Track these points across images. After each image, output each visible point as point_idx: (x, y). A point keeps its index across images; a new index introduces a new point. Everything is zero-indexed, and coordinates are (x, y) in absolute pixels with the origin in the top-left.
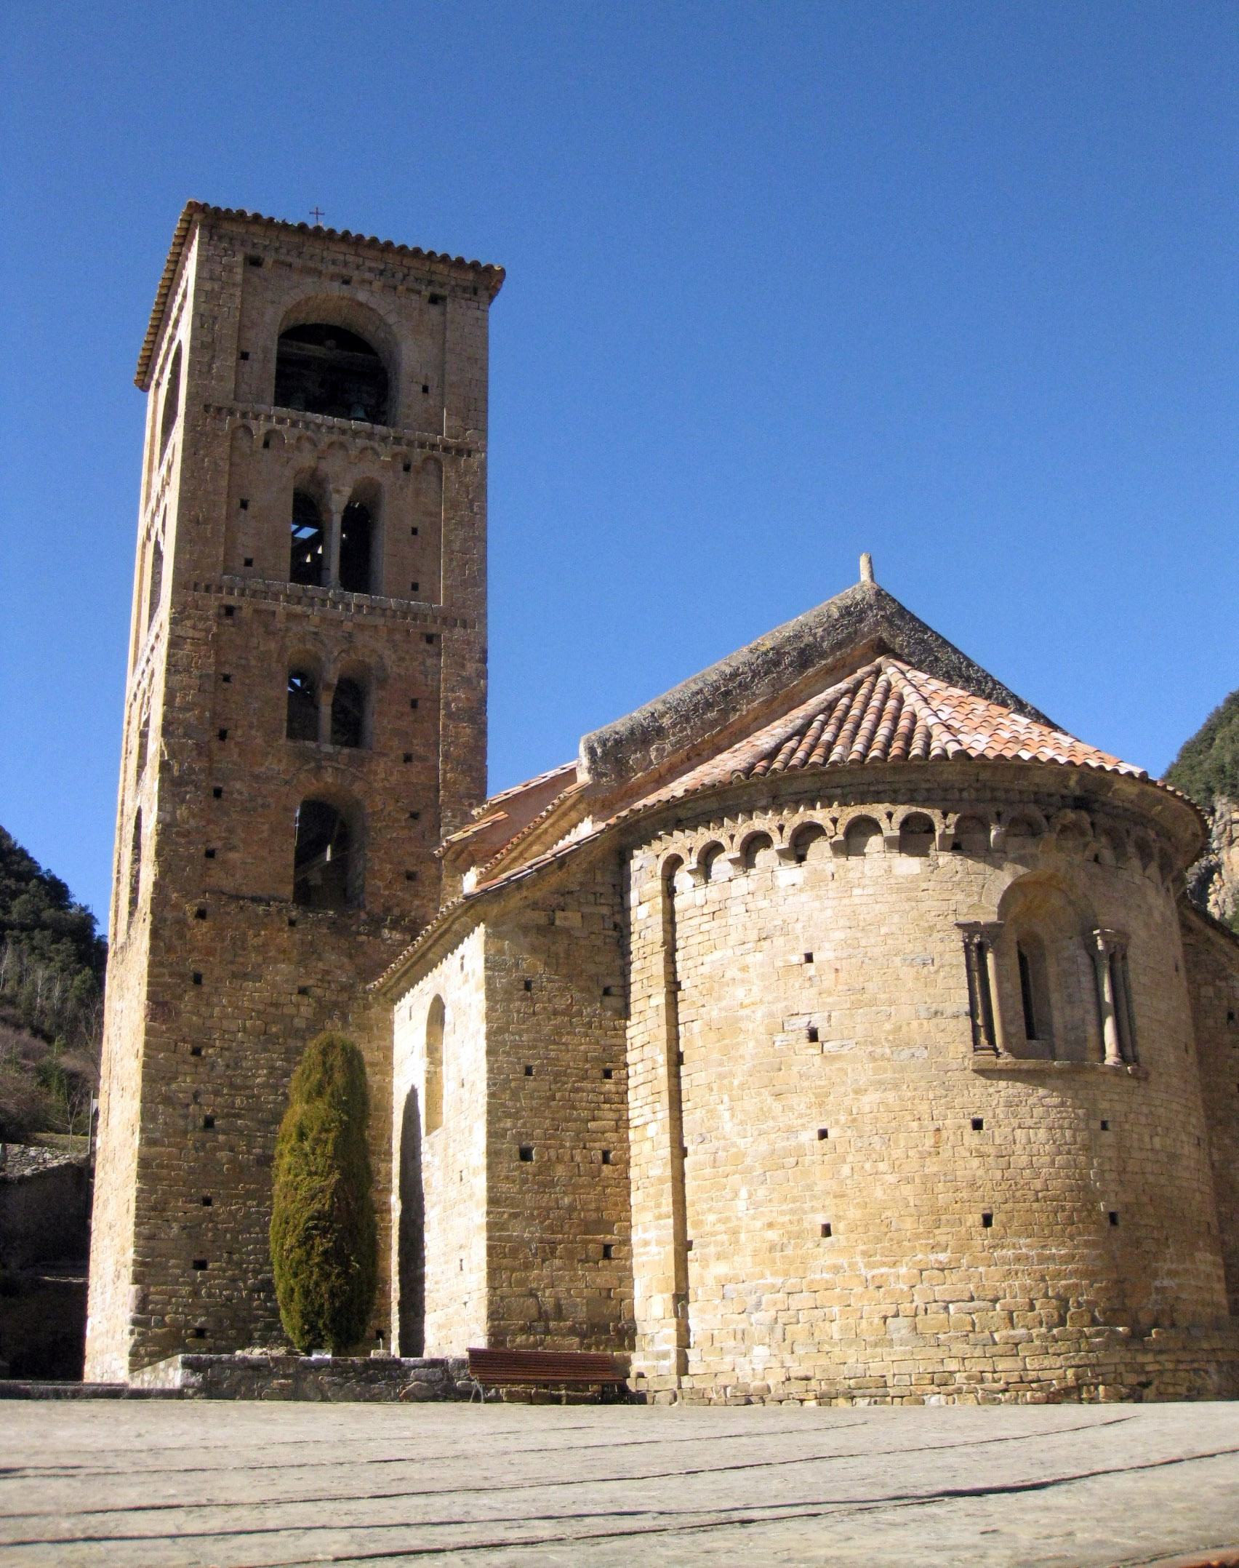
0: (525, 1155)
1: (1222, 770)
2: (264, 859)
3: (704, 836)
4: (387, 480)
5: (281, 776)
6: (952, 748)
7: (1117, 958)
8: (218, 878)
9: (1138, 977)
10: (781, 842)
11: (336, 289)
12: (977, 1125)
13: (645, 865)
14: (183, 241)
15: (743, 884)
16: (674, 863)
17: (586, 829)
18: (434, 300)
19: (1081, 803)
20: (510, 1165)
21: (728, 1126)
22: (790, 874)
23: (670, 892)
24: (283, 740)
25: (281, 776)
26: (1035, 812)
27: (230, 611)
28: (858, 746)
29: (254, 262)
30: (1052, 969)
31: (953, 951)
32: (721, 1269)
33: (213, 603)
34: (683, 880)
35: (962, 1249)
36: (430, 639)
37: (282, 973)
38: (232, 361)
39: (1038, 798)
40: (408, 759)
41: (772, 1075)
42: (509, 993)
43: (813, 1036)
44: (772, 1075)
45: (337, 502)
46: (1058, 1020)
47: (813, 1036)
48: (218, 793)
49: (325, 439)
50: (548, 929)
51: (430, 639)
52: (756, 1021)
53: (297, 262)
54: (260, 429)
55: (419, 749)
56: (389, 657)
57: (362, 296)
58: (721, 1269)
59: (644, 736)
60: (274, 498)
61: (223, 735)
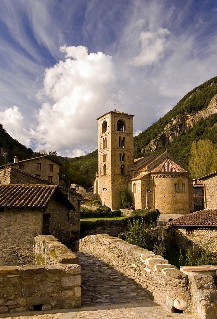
0: (144, 196)
1: (186, 107)
2: (118, 171)
3: (156, 175)
4: (126, 137)
5: (119, 164)
6: (175, 171)
7: (184, 185)
8: (116, 173)
9: (185, 186)
10: (162, 176)
11: (121, 118)
12: (175, 196)
13: (152, 176)
14: (109, 113)
15: (159, 179)
16: (154, 176)
17: (147, 173)
18: (129, 119)
19: (183, 174)
20: (143, 197)
21: (158, 195)
22: (163, 178)
23: (154, 178)
24: (119, 161)
25: (119, 164)
26: (180, 175)
27: (115, 150)
28: (168, 170)
29: (115, 116)
30: (180, 185)
31: (174, 184)
32: (157, 205)
33: (114, 149)
34: (155, 178)
35: (174, 204)
36: (129, 151)
37: (120, 180)
38: (114, 126)
39: (180, 174)
40: (128, 162)
41: (161, 192)
42: (143, 185)
43: (164, 190)
44: (161, 192)
45: (122, 139)
46: (180, 189)
47: (164, 190)
48: (115, 166)
49: (121, 133)
50: (145, 180)
51: (129, 151)
52: (160, 189)
53: (118, 116)
54: (116, 133)
55: (129, 161)
56: (127, 153)
57: (123, 119)
58: (157, 205)
59: (151, 165)
60: (118, 140)
61: (115, 161)
